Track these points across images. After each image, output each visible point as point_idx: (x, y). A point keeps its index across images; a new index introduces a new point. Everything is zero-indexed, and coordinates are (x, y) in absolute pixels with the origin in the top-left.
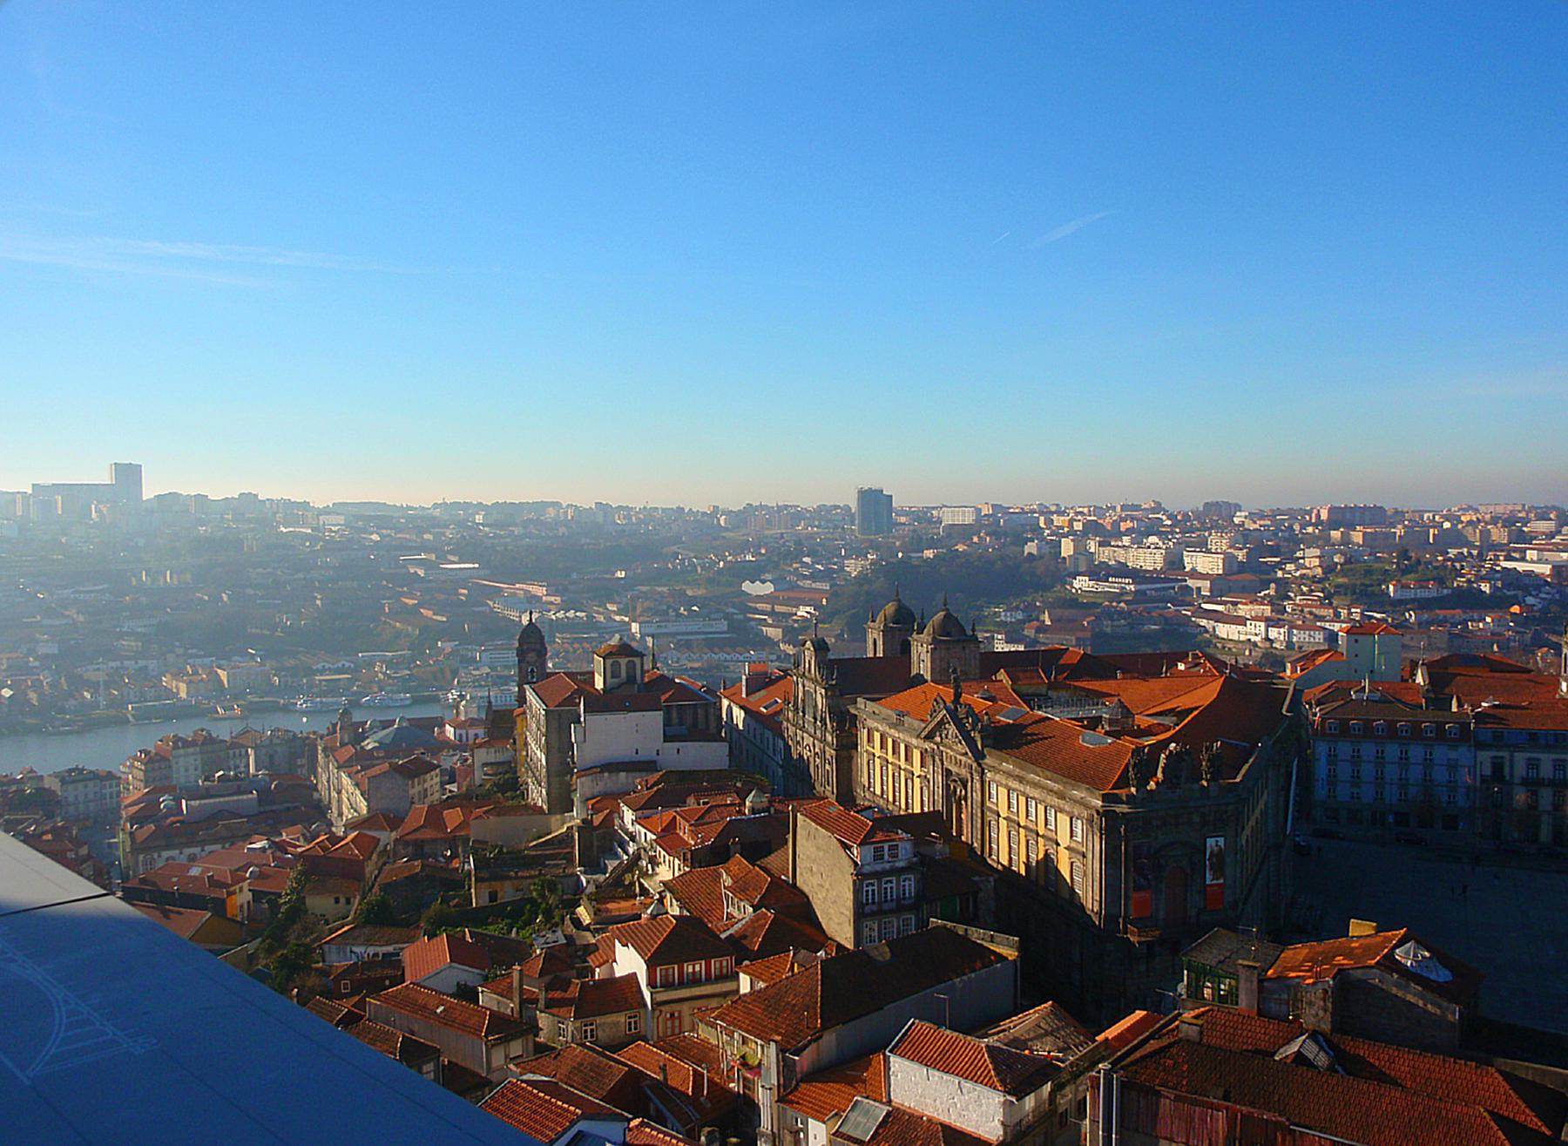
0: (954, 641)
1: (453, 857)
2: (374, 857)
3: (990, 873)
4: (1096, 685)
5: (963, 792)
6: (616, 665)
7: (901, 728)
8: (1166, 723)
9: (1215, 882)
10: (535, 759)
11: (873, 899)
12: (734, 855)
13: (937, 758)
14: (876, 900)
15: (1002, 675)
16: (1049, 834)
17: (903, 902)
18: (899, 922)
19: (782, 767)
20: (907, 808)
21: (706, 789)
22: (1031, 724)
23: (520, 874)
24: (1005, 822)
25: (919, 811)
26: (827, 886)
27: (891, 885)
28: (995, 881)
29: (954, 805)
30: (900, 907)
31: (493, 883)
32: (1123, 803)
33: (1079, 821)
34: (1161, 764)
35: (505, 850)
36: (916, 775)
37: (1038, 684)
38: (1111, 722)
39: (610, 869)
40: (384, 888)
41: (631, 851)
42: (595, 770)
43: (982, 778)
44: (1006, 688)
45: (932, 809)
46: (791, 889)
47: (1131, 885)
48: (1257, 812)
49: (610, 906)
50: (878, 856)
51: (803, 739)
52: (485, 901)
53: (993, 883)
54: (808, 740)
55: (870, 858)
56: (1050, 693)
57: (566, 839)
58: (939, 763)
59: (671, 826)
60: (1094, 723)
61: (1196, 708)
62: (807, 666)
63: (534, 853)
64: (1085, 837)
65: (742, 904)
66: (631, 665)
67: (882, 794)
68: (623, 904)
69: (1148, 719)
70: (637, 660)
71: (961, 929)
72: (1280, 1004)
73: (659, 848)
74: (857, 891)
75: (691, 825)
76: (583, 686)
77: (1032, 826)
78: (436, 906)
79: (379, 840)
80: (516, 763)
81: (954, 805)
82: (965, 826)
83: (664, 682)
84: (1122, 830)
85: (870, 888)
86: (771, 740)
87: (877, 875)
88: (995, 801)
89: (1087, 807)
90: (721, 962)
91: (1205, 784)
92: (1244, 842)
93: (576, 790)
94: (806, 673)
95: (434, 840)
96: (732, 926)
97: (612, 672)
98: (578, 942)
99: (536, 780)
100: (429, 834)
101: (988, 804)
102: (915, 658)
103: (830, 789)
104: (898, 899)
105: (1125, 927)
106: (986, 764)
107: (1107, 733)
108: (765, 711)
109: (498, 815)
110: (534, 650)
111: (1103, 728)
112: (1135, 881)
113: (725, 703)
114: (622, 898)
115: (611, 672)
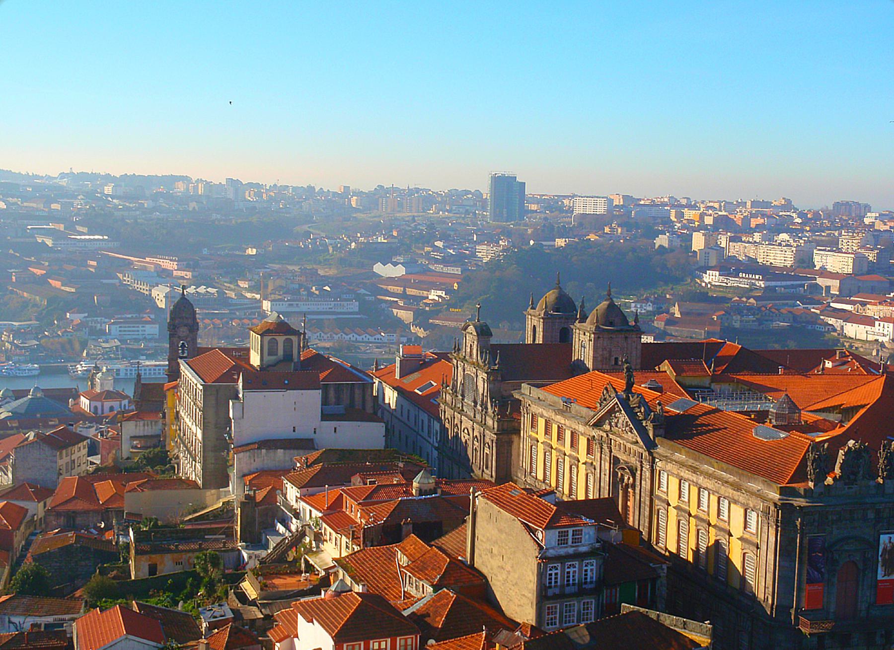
0: (617, 331)
1: (109, 527)
2: (22, 528)
3: (663, 561)
4: (758, 379)
5: (631, 479)
6: (273, 345)
7: (569, 415)
8: (831, 419)
9: (886, 578)
10: (188, 432)
11: (556, 582)
12: (407, 535)
13: (605, 446)
14: (559, 584)
15: (666, 366)
16: (721, 524)
17: (584, 586)
18: (580, 606)
19: (437, 449)
20: (570, 494)
21: (368, 469)
22: (701, 416)
23: (180, 547)
24: (675, 511)
25: (583, 498)
26: (508, 567)
27: (574, 570)
28: (668, 567)
29: (621, 492)
30: (581, 591)
31: (153, 556)
32: (801, 497)
33: (754, 515)
34: (840, 460)
35: (160, 523)
36: (582, 461)
37: (704, 376)
38: (778, 416)
39: (272, 545)
40: (37, 558)
41: (293, 528)
42: (252, 446)
43: (652, 467)
44: (669, 378)
45: (598, 497)
46: (470, 570)
47: (805, 577)
49: (277, 581)
50: (562, 541)
51: (461, 422)
52: (145, 573)
53: (665, 571)
54: (467, 423)
55: (554, 542)
56: (713, 386)
57: (225, 513)
58: (607, 450)
59: (337, 504)
60: (761, 417)
61: (863, 406)
62: (469, 350)
63: (190, 527)
65: (421, 583)
67: (544, 479)
68: (291, 580)
69: (810, 414)
70: (294, 338)
71: (653, 614)
73: (324, 525)
74: (541, 575)
75: (359, 504)
76: (239, 362)
77: (704, 516)
78: (96, 579)
79: (27, 510)
80: (165, 437)
81: (621, 492)
82: (631, 513)
83: (318, 361)
84: (798, 523)
85: (553, 572)
86: (426, 422)
88: (665, 490)
89: (764, 499)
90: (406, 639)
91: (880, 480)
93: (232, 465)
94: (467, 357)
95: (86, 512)
96: (412, 605)
97: (269, 349)
98: (245, 617)
99: (191, 454)
100: (80, 505)
101: (657, 492)
102: (576, 346)
103: (488, 472)
104: (580, 584)
105: (796, 618)
106: (657, 453)
107: (774, 426)
108: (420, 393)
109: (153, 489)
110: (185, 325)
111: (770, 423)
112: (808, 573)
113: (376, 381)
114: (286, 574)
115: (268, 350)
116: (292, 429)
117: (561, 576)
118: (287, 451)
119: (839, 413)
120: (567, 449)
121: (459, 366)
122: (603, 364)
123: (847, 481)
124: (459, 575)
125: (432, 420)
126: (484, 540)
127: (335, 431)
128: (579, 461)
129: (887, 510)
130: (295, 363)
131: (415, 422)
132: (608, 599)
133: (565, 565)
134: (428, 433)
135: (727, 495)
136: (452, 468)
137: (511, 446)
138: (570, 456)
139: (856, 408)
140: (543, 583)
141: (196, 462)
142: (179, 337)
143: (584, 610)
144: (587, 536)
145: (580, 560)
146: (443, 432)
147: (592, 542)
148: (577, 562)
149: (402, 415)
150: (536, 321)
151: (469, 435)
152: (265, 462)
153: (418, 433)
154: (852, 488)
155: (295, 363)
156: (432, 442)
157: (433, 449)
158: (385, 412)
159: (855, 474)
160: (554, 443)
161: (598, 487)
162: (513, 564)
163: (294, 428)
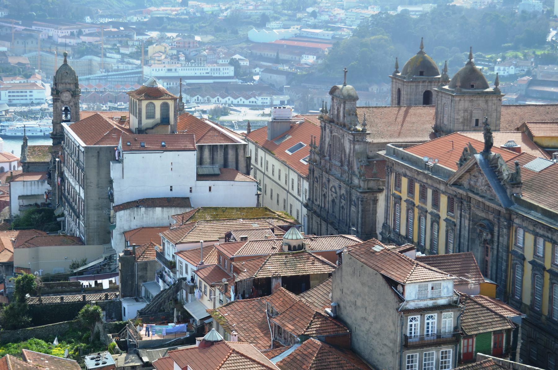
19: (306, 206)
26: (371, 319)
51: (329, 181)
54: (334, 183)
62: (336, 113)
66: (165, 107)
110: (68, 90)
116: (169, 188)
118: (165, 209)
120: (429, 207)
121: (327, 128)
122: (464, 126)
124: (325, 325)
125: (302, 179)
126: (349, 293)
127: (210, 190)
128: (439, 218)
130: (171, 126)
131: (286, 181)
132: (465, 348)
133: (424, 315)
134: (298, 192)
136: (321, 225)
137: (376, 204)
140: (403, 333)
141: (79, 220)
142: (62, 102)
143: (442, 358)
144: (445, 290)
145: (438, 311)
146: (312, 191)
147: (451, 294)
148: (436, 314)
149: (273, 175)
150: (400, 85)
151: (336, 193)
152: (145, 219)
153: (288, 192)
155: (171, 126)
156: (301, 200)
157: (303, 206)
158: (258, 171)
160: (417, 201)
161: (458, 243)
162: (375, 316)
163: (171, 187)
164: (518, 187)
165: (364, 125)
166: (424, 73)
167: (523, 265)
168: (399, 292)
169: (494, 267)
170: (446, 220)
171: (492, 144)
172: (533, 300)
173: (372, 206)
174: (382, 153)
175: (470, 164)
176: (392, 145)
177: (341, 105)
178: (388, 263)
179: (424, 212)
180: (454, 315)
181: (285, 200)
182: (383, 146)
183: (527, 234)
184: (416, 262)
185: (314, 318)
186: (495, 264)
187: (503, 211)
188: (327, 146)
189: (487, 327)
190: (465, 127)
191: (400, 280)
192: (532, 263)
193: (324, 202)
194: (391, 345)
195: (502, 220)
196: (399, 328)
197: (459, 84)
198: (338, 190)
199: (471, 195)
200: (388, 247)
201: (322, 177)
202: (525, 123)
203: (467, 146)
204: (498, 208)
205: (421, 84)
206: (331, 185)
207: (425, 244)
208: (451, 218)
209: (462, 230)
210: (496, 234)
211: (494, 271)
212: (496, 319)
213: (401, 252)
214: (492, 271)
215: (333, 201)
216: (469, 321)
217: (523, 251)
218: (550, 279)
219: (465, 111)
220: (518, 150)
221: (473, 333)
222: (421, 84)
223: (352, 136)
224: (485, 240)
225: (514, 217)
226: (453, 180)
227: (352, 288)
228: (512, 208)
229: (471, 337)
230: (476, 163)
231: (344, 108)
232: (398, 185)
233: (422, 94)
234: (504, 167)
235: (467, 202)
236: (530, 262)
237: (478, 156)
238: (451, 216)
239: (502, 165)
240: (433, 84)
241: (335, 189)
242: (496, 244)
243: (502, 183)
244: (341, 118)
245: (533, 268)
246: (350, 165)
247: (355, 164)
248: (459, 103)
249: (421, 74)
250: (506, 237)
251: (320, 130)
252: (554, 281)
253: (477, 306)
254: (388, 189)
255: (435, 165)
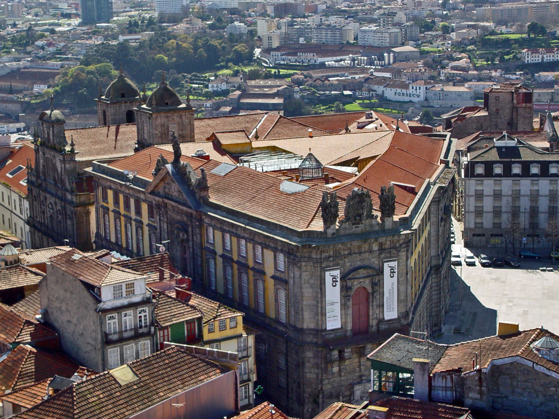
5: (186, 236)
16: (257, 267)
19: (28, 223)
26: (75, 321)
48: (422, 241)
51: (46, 198)
61: (373, 158)
62: (46, 136)
64: (287, 267)
72: (446, 391)
87: (118, 309)
92: (412, 265)
104: (136, 329)
117: (119, 325)
119: (356, 166)
120: (133, 215)
123: (354, 222)
129: (388, 242)
133: (121, 313)
135: (260, 241)
136: (42, 239)
137: (89, 216)
138: (135, 220)
139: (367, 160)
144: (139, 288)
145: (134, 308)
151: (53, 209)
153: (12, 212)
154: (358, 227)
159: (360, 215)
160: (122, 211)
164: (205, 191)
165: (72, 145)
166: (126, 95)
167: (215, 259)
168: (96, 294)
169: (192, 263)
170: (148, 225)
171: (180, 154)
172: (226, 289)
173: (85, 217)
174: (89, 170)
175: (162, 173)
176: (98, 162)
177: (50, 129)
178: (86, 269)
179: (128, 219)
180: (149, 310)
181: (9, 219)
182: (89, 163)
183: (216, 231)
184: (110, 266)
185: (24, 326)
186: (192, 260)
187: (194, 213)
188: (41, 167)
189: (180, 317)
190: (164, 141)
191: (96, 284)
192: (222, 256)
193: (44, 218)
194: (93, 343)
195: (194, 221)
196: (99, 328)
197: (154, 102)
198: (54, 206)
199: (166, 201)
200: (86, 254)
201: (40, 196)
202: (213, 133)
203: (159, 158)
204: (189, 210)
205: (123, 105)
206: (48, 203)
207: (132, 248)
208: (152, 223)
209: (162, 232)
210: (190, 234)
211: (192, 267)
212: (188, 310)
213: (98, 258)
214: (190, 267)
215: (51, 216)
216: (162, 314)
217: (214, 247)
218: (238, 269)
219: (162, 126)
220: (207, 158)
221: (167, 324)
222: (123, 105)
223: (62, 157)
224: (182, 240)
225: (204, 217)
226: (150, 189)
227: (57, 295)
228: (201, 209)
229: (166, 327)
230: (168, 172)
231: (53, 132)
232: (105, 198)
233: (125, 113)
234: (192, 173)
235: (164, 207)
236: (220, 256)
237: (169, 167)
238: (152, 221)
239: (190, 172)
240: (134, 104)
241: (52, 206)
242: (191, 243)
243: (191, 188)
244: (52, 141)
245: (223, 261)
246: (62, 182)
247: (67, 181)
248: (156, 120)
249: (123, 96)
250: (199, 236)
251: (34, 153)
252: (241, 271)
253: (170, 300)
254: (97, 201)
255: (134, 176)
